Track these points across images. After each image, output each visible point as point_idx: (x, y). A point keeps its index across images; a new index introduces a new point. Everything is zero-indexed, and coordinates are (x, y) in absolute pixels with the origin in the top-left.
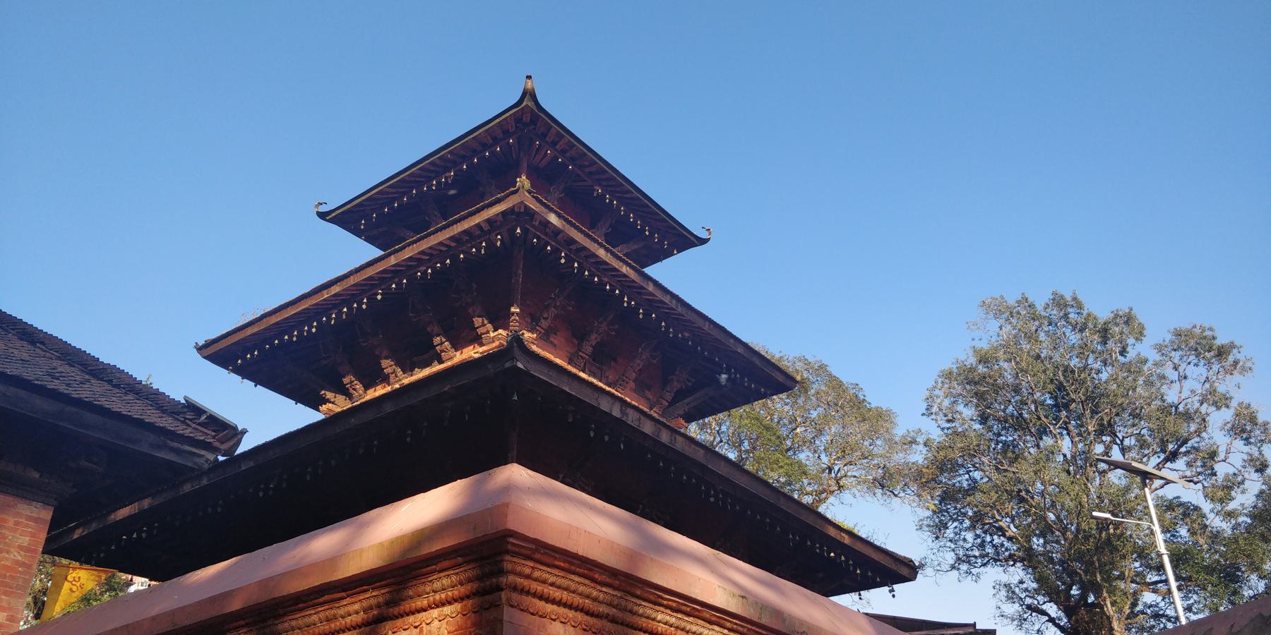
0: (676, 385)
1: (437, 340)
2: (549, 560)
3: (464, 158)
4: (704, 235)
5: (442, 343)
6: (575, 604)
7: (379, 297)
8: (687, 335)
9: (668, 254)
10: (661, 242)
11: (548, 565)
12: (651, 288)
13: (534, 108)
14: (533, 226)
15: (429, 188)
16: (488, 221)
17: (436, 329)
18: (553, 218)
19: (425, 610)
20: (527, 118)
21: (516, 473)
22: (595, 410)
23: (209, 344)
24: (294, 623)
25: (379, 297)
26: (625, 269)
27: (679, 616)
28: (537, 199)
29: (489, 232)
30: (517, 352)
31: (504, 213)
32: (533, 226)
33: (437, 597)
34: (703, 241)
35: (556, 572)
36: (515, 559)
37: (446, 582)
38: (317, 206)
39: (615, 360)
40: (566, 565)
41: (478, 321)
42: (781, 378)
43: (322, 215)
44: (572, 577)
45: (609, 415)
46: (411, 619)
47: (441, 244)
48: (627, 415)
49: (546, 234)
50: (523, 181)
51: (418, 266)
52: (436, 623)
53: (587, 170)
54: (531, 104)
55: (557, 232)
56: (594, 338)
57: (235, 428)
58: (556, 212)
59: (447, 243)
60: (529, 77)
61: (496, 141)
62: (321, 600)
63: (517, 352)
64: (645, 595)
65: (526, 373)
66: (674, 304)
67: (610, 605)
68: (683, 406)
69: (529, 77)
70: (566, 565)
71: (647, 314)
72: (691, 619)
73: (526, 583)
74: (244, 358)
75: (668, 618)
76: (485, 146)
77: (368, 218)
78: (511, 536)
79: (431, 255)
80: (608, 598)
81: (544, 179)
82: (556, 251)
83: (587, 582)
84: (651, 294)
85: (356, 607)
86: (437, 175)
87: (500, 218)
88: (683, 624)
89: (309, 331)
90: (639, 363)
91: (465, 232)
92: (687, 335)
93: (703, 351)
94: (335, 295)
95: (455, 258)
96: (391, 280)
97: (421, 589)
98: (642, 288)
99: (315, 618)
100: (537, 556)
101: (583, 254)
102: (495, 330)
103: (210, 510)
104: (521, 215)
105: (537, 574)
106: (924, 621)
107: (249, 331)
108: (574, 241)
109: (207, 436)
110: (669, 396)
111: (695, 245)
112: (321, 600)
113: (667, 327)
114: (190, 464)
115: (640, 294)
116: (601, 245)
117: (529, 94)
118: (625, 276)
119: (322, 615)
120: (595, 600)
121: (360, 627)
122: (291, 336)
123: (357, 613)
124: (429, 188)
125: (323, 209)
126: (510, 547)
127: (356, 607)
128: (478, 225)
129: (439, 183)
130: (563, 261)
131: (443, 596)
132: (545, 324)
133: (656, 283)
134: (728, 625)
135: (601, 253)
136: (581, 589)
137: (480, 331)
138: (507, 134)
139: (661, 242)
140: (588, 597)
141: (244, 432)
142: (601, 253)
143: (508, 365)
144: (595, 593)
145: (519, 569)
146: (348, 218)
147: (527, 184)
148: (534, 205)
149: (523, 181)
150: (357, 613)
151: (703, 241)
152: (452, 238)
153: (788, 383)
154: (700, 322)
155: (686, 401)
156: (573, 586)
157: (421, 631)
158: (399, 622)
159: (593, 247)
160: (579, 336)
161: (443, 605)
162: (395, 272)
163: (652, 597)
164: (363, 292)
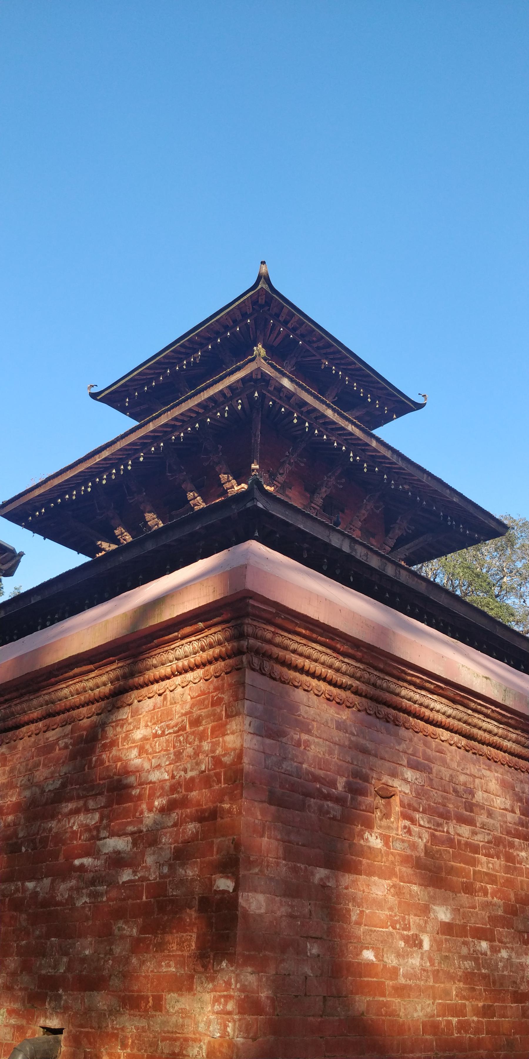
0: (397, 532)
1: (190, 495)
2: (290, 626)
3: (209, 340)
4: (420, 400)
5: (195, 498)
6: (318, 672)
7: (141, 459)
8: (406, 487)
9: (389, 419)
10: (381, 408)
11: (289, 632)
12: (374, 444)
13: (268, 290)
14: (269, 392)
15: (181, 368)
17: (190, 486)
18: (286, 383)
19: (168, 678)
20: (262, 301)
21: (255, 546)
22: (327, 546)
24: (47, 697)
25: (141, 459)
26: (350, 428)
27: (423, 693)
28: (271, 365)
29: (231, 398)
30: (257, 494)
31: (243, 380)
33: (180, 664)
34: (419, 406)
35: (298, 639)
36: (255, 623)
37: (188, 648)
38: (89, 388)
39: (343, 511)
40: (307, 633)
41: (223, 477)
42: (493, 525)
43: (94, 396)
44: (314, 645)
45: (339, 550)
46: (155, 687)
47: (190, 410)
48: (356, 550)
49: (280, 398)
50: (259, 350)
51: (172, 432)
52: (179, 689)
53: (315, 345)
54: (265, 287)
55: (290, 395)
56: (324, 491)
57: (12, 551)
59: (196, 409)
60: (263, 263)
61: (236, 322)
62: (71, 673)
63: (257, 494)
64: (388, 669)
65: (264, 513)
66: (394, 459)
67: (352, 676)
68: (405, 551)
69: (263, 263)
70: (307, 633)
71: (371, 469)
72: (435, 697)
73: (266, 647)
74: (34, 516)
75: (412, 694)
76: (227, 328)
77: (131, 396)
78: (251, 598)
79: (183, 421)
80: (351, 670)
81: (276, 353)
82: (289, 414)
83: (329, 651)
84: (375, 450)
85: (104, 678)
86: (188, 356)
87: (240, 385)
88: (427, 702)
89: (85, 491)
90: (364, 513)
91: (211, 399)
92: (406, 487)
93: (422, 500)
94: (105, 459)
95: (202, 423)
96: (151, 444)
97: (164, 657)
98: (367, 445)
99: (66, 691)
100: (279, 621)
101: (313, 415)
102: (239, 484)
104: (258, 380)
105: (278, 640)
108: (305, 403)
110: (392, 543)
111: (412, 410)
112: (71, 673)
113: (389, 480)
115: (363, 450)
116: (328, 406)
117: (263, 278)
118: (351, 434)
119: (72, 688)
120: (338, 670)
121: (108, 698)
122: (71, 495)
123: (105, 684)
124: (181, 368)
125: (95, 390)
126: (250, 609)
127: (104, 678)
128: (221, 391)
129: (188, 363)
130: (295, 421)
131: (186, 663)
132: (281, 478)
133: (378, 440)
134: (472, 705)
135: (329, 413)
136: (323, 658)
137: (227, 486)
138: (245, 316)
139: (381, 408)
140: (330, 667)
141: (21, 554)
142: (329, 413)
143: (249, 505)
144: (337, 664)
145: (260, 633)
146: (114, 397)
147: (263, 352)
148: (269, 371)
149: (259, 350)
150: (105, 684)
151: (419, 406)
152: (199, 405)
153: (500, 529)
154: (418, 475)
155: (407, 547)
156: (315, 655)
157: (165, 699)
158: (144, 691)
159: (321, 408)
160: (311, 490)
161: (186, 671)
162: (153, 437)
163: (395, 672)
164: (128, 457)
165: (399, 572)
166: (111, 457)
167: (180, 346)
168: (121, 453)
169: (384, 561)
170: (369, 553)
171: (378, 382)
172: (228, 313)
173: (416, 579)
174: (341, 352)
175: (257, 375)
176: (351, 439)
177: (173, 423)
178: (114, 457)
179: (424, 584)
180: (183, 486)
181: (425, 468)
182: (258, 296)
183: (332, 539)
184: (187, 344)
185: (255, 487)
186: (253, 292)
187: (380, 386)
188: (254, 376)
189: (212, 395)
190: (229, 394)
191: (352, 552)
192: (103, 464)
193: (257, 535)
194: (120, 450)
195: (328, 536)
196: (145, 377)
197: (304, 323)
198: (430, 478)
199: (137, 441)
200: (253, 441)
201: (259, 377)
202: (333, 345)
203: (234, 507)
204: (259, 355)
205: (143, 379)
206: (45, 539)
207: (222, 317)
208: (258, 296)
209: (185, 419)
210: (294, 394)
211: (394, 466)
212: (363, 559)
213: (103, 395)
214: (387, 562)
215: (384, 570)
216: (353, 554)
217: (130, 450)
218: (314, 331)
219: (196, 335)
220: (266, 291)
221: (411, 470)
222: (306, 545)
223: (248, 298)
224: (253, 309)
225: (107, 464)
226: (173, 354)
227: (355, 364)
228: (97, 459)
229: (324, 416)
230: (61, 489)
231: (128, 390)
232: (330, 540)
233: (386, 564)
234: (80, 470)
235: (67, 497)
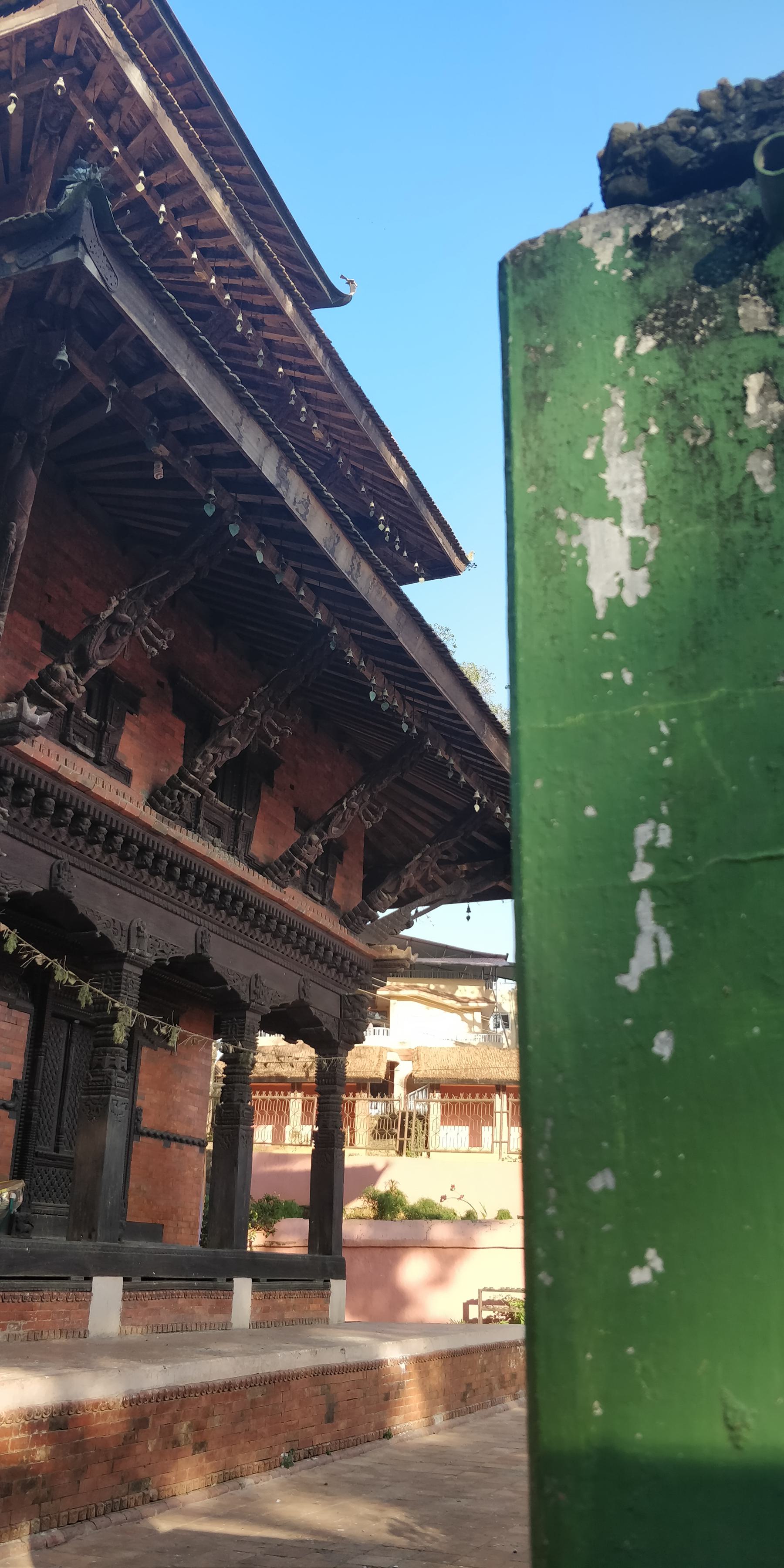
14: (85, 102)
18: (135, 77)
30: (88, 229)
32: (85, 102)
48: (287, 484)
49: (108, 130)
58: (143, 68)
87: (19, 55)
98: (278, 310)
106: (447, 947)
118: (249, 272)
143: (60, 257)
153: (456, 561)
165: (359, 565)
169: (337, 530)
170: (313, 501)
171: (280, 225)
173: (384, 592)
174: (222, 126)
176: (242, 289)
179: (395, 607)
181: (368, 397)
183: (244, 434)
185: (87, 204)
187: (278, 231)
188: (58, 45)
191: (279, 485)
193: (65, 358)
195: (238, 425)
197: (159, 24)
198: (370, 423)
202: (208, 104)
203: (9, 259)
210: (148, 118)
211: (309, 377)
212: (297, 510)
214: (341, 534)
215: (333, 551)
216: (281, 490)
218: (176, 52)
221: (343, 393)
222: (162, 450)
227: (242, 164)
229: (204, 205)
232: (241, 437)
233: (339, 539)
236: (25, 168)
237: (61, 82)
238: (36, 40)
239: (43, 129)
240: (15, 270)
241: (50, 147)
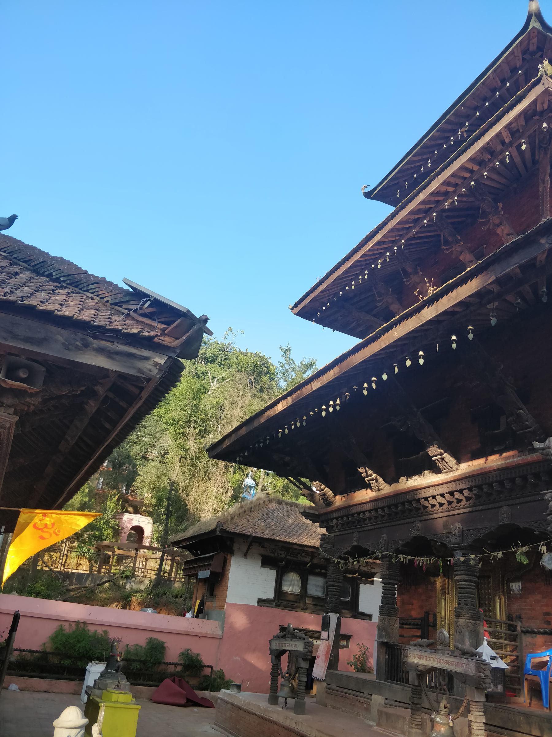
13: (540, 28)
16: (508, 127)
23: (296, 305)
29: (511, 144)
43: (368, 195)
47: (463, 168)
51: (445, 201)
54: (537, 25)
79: (456, 185)
86: (454, 132)
87: (522, 122)
91: (486, 148)
94: (378, 243)
103: (298, 424)
107: (321, 288)
109: (154, 329)
114: (132, 372)
146: (384, 193)
166: (384, 240)
167: (445, 122)
168: (394, 234)
172: (495, 71)
175: (543, 104)
177: (444, 189)
178: (387, 240)
180: (461, 258)
182: (529, 42)
184: (453, 119)
186: (522, 37)
189: (488, 143)
190: (507, 138)
192: (377, 250)
194: (392, 230)
196: (413, 166)
199: (409, 217)
200: (541, 190)
201: (546, 106)
203: (543, 241)
204: (546, 74)
205: (412, 168)
206: (334, 331)
207: (489, 77)
208: (529, 42)
209: (459, 181)
213: (376, 192)
217: (403, 229)
219: (462, 105)
220: (539, 31)
223: (517, 46)
224: (524, 59)
225: (381, 249)
226: (438, 133)
228: (371, 244)
230: (342, 282)
231: (398, 183)
234: (356, 259)
235: (347, 288)
236: (534, 162)
237: (545, 125)
238: (528, 111)
239: (540, 147)
240: (547, 246)
241: (546, 154)
